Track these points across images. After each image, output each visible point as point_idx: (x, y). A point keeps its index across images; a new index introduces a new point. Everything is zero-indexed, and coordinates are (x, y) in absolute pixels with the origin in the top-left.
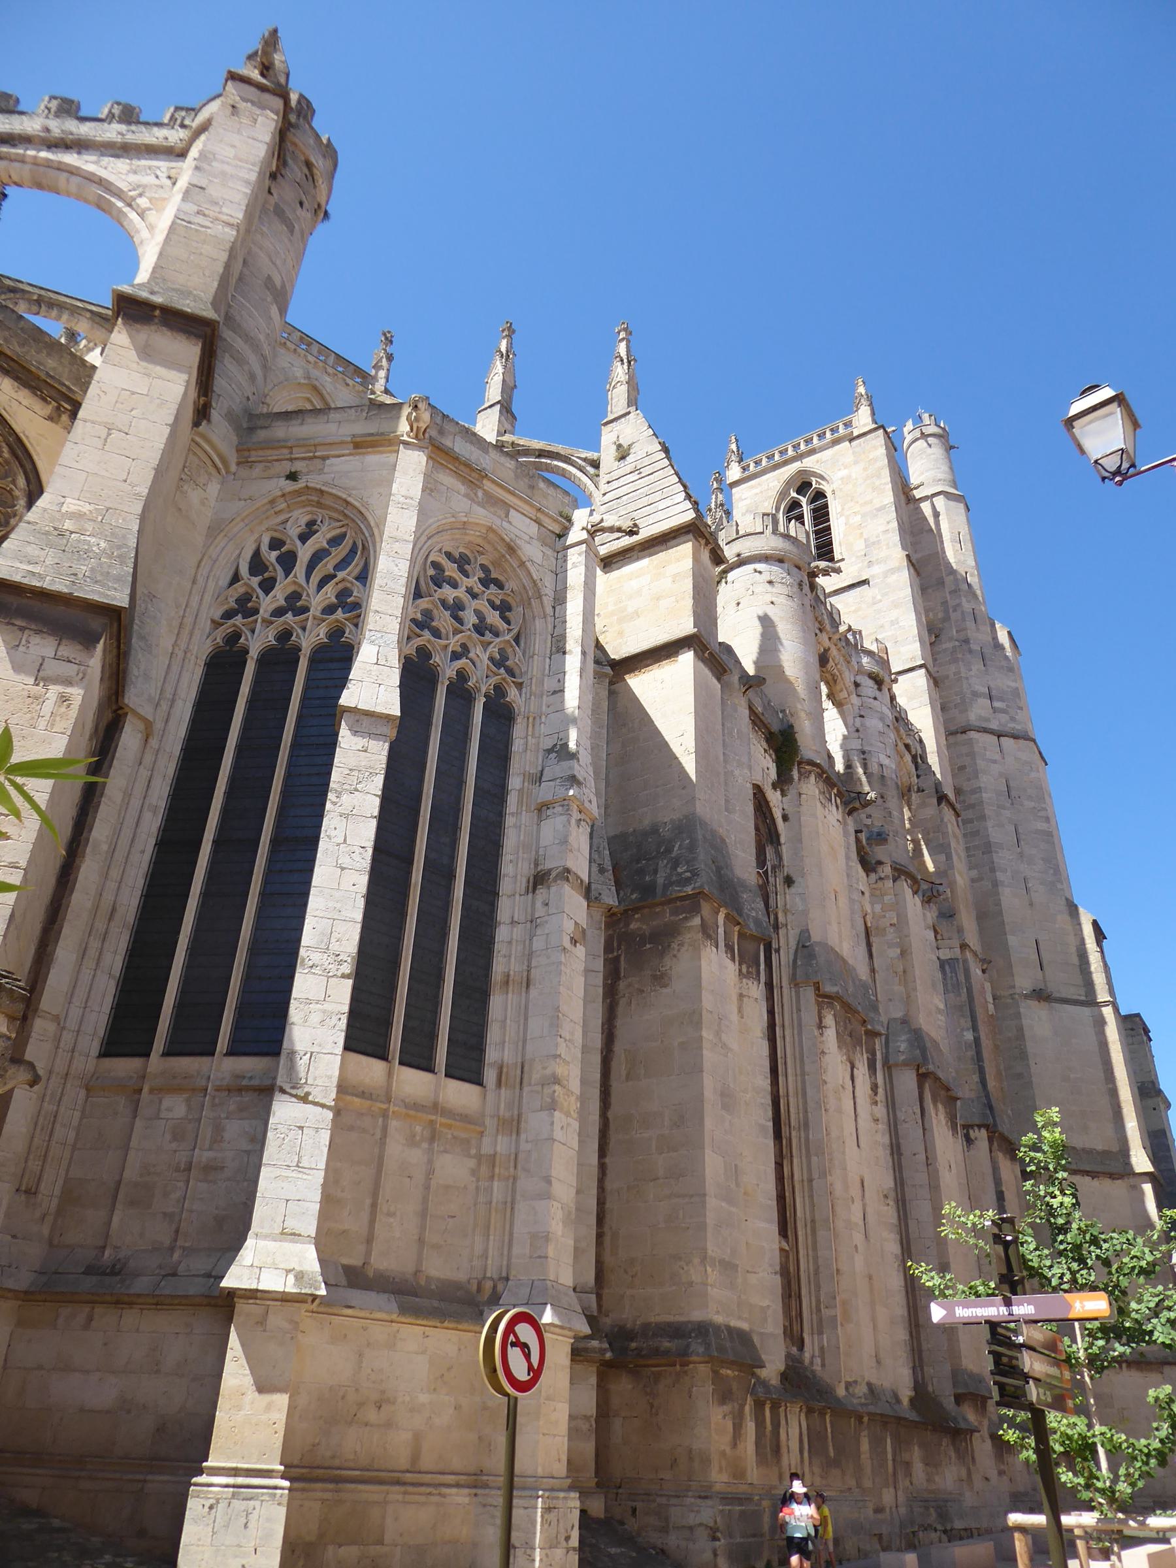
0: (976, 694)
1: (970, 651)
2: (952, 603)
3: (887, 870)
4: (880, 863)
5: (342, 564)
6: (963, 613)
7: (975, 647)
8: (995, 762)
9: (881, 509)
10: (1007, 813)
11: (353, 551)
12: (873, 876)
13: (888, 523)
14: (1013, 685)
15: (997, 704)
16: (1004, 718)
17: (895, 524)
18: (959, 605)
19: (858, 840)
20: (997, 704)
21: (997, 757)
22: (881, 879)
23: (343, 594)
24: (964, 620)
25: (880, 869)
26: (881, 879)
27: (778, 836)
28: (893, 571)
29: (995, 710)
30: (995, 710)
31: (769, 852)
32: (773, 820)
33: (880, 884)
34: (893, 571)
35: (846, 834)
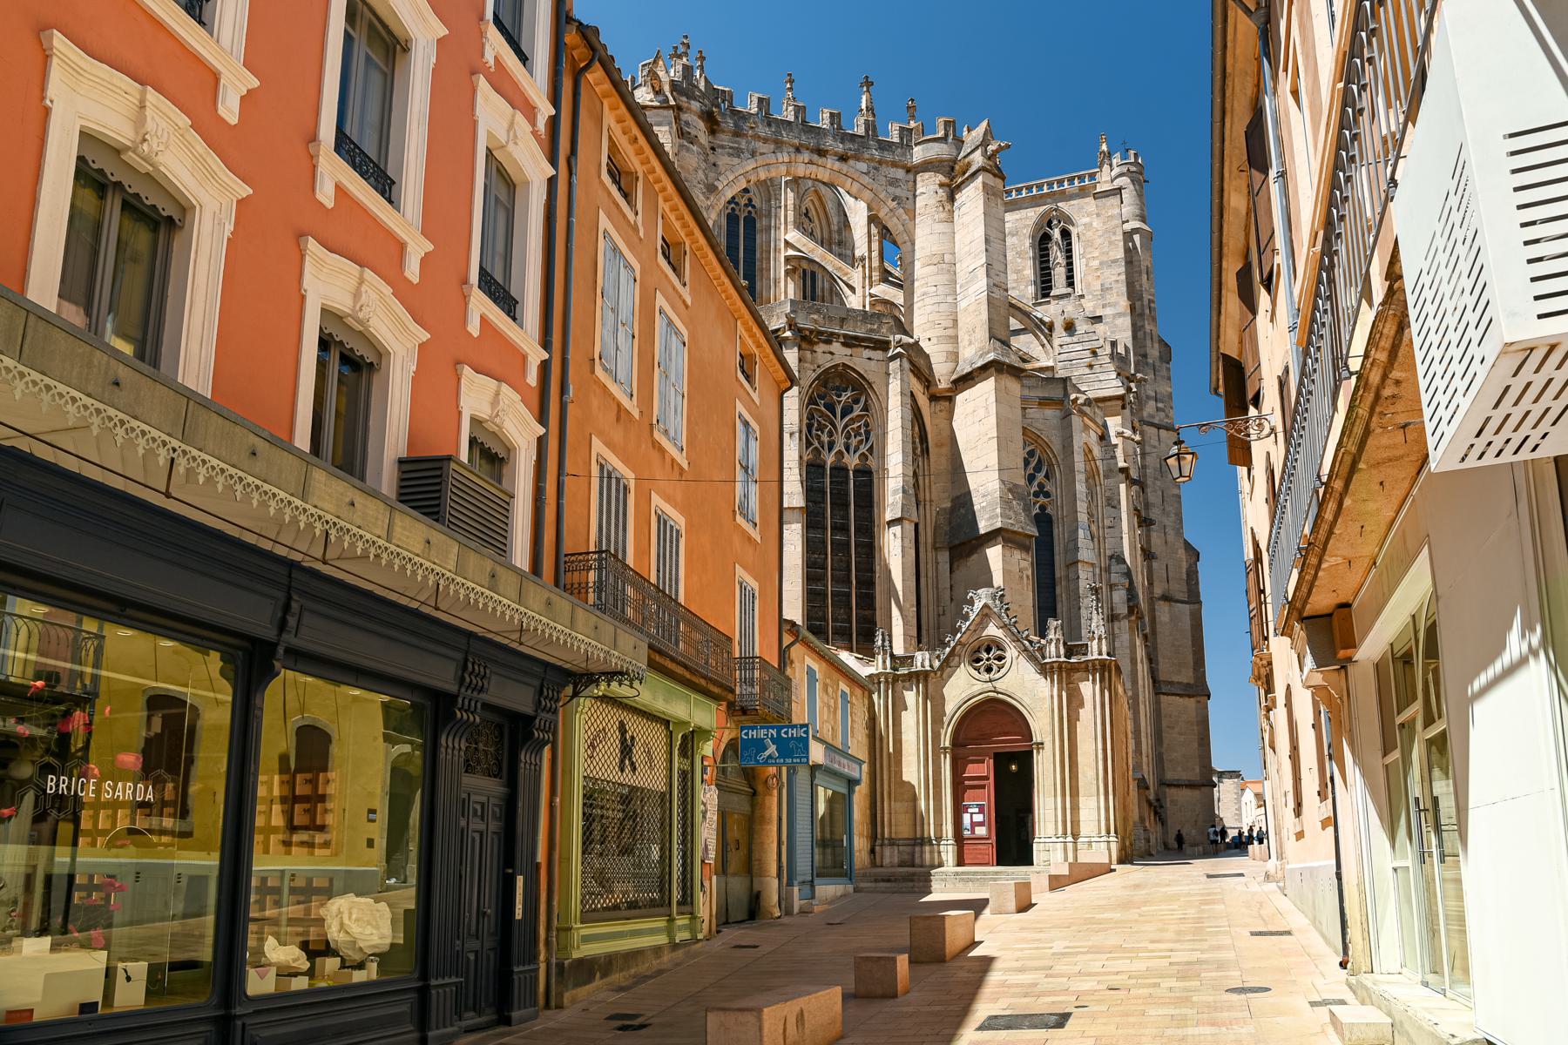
0: (1148, 397)
1: (1147, 364)
2: (1139, 324)
5: (1038, 469)
6: (1145, 333)
7: (1150, 361)
8: (1155, 447)
10: (1158, 483)
11: (1040, 461)
14: (1169, 389)
15: (1160, 405)
16: (1162, 414)
17: (1123, 277)
18: (1143, 326)
20: (1160, 405)
21: (1156, 444)
23: (1041, 486)
24: (1145, 339)
29: (1158, 409)
30: (1158, 409)
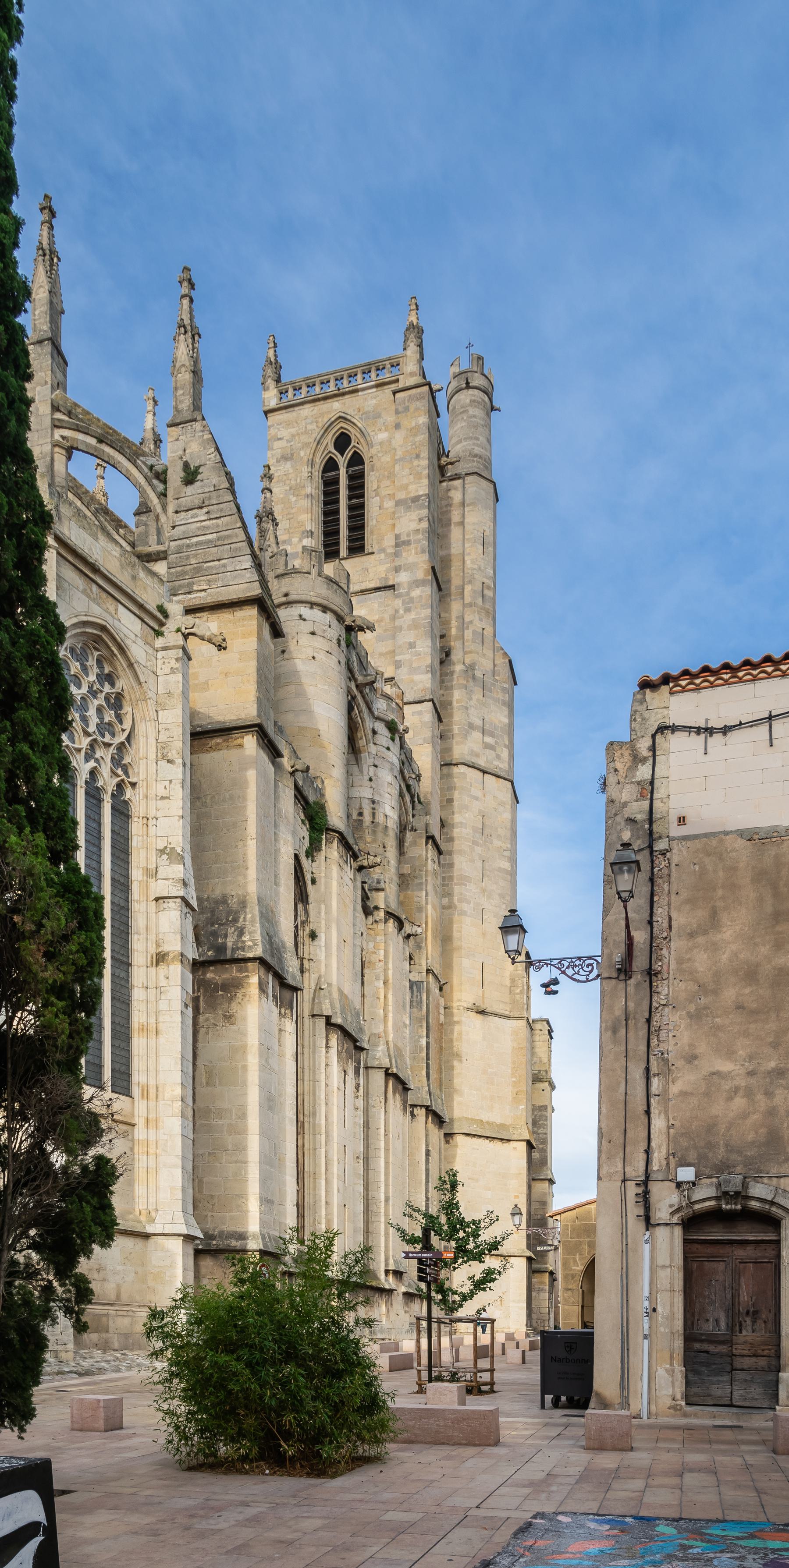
3: (382, 914)
4: (377, 908)
9: (415, 499)
12: (371, 919)
13: (420, 520)
19: (363, 888)
22: (376, 921)
25: (376, 913)
26: (376, 921)
27: (307, 896)
28: (417, 583)
31: (300, 907)
32: (305, 883)
33: (375, 926)
34: (417, 583)
35: (355, 887)
